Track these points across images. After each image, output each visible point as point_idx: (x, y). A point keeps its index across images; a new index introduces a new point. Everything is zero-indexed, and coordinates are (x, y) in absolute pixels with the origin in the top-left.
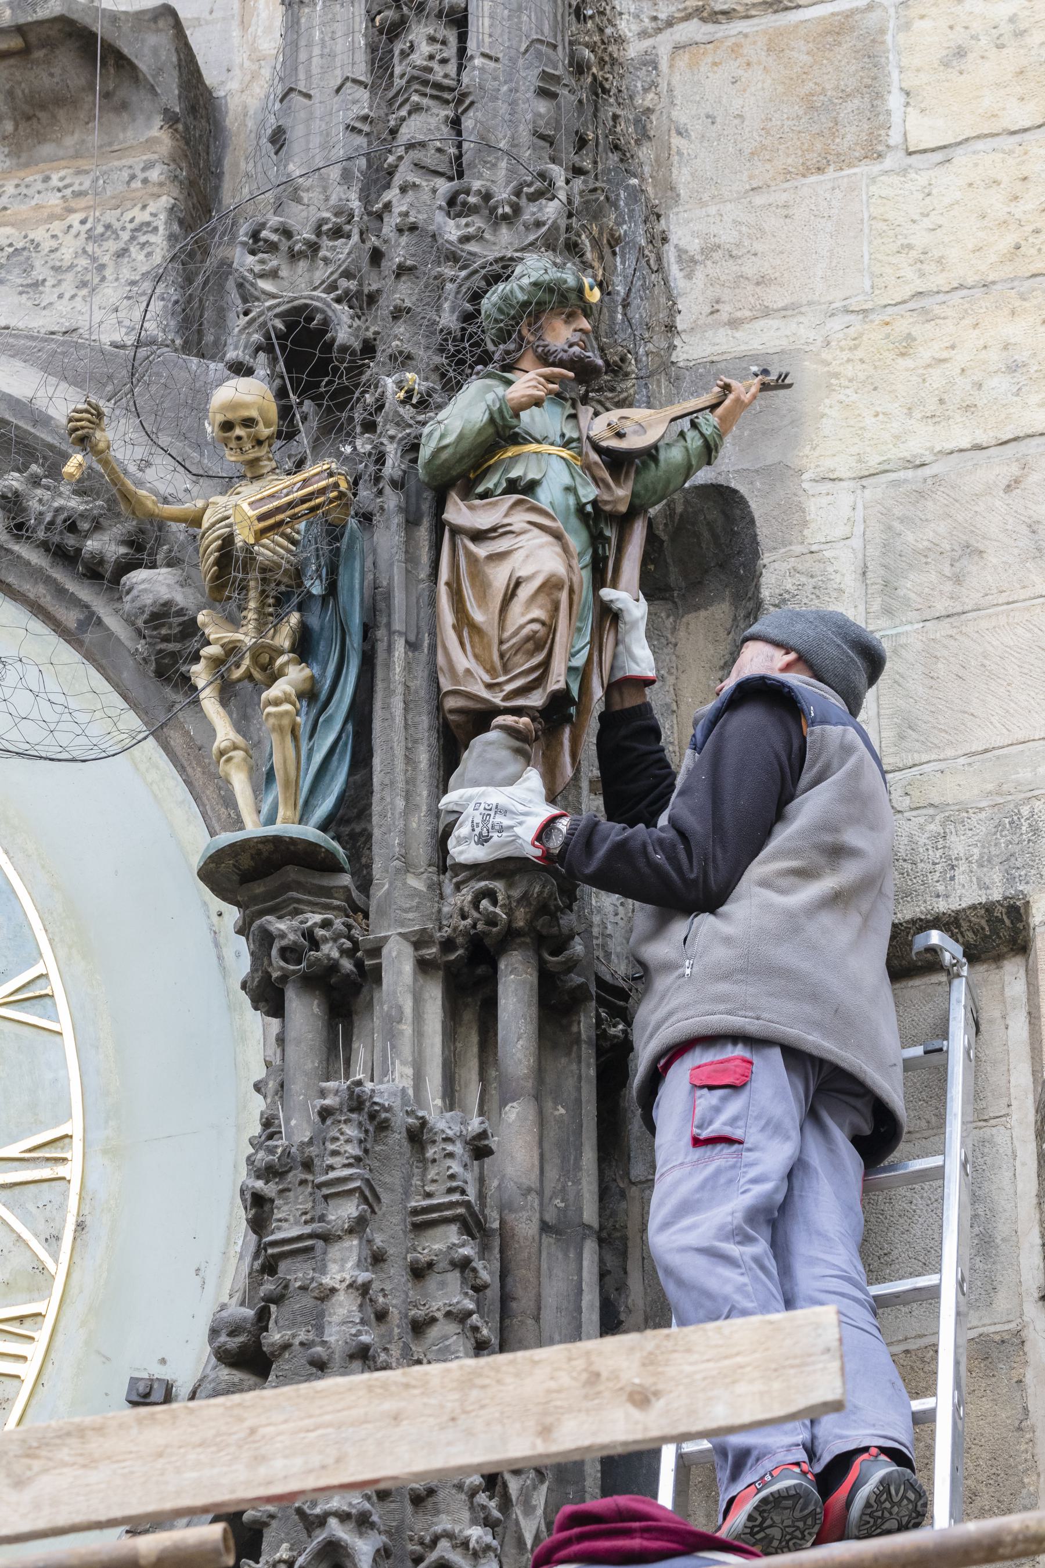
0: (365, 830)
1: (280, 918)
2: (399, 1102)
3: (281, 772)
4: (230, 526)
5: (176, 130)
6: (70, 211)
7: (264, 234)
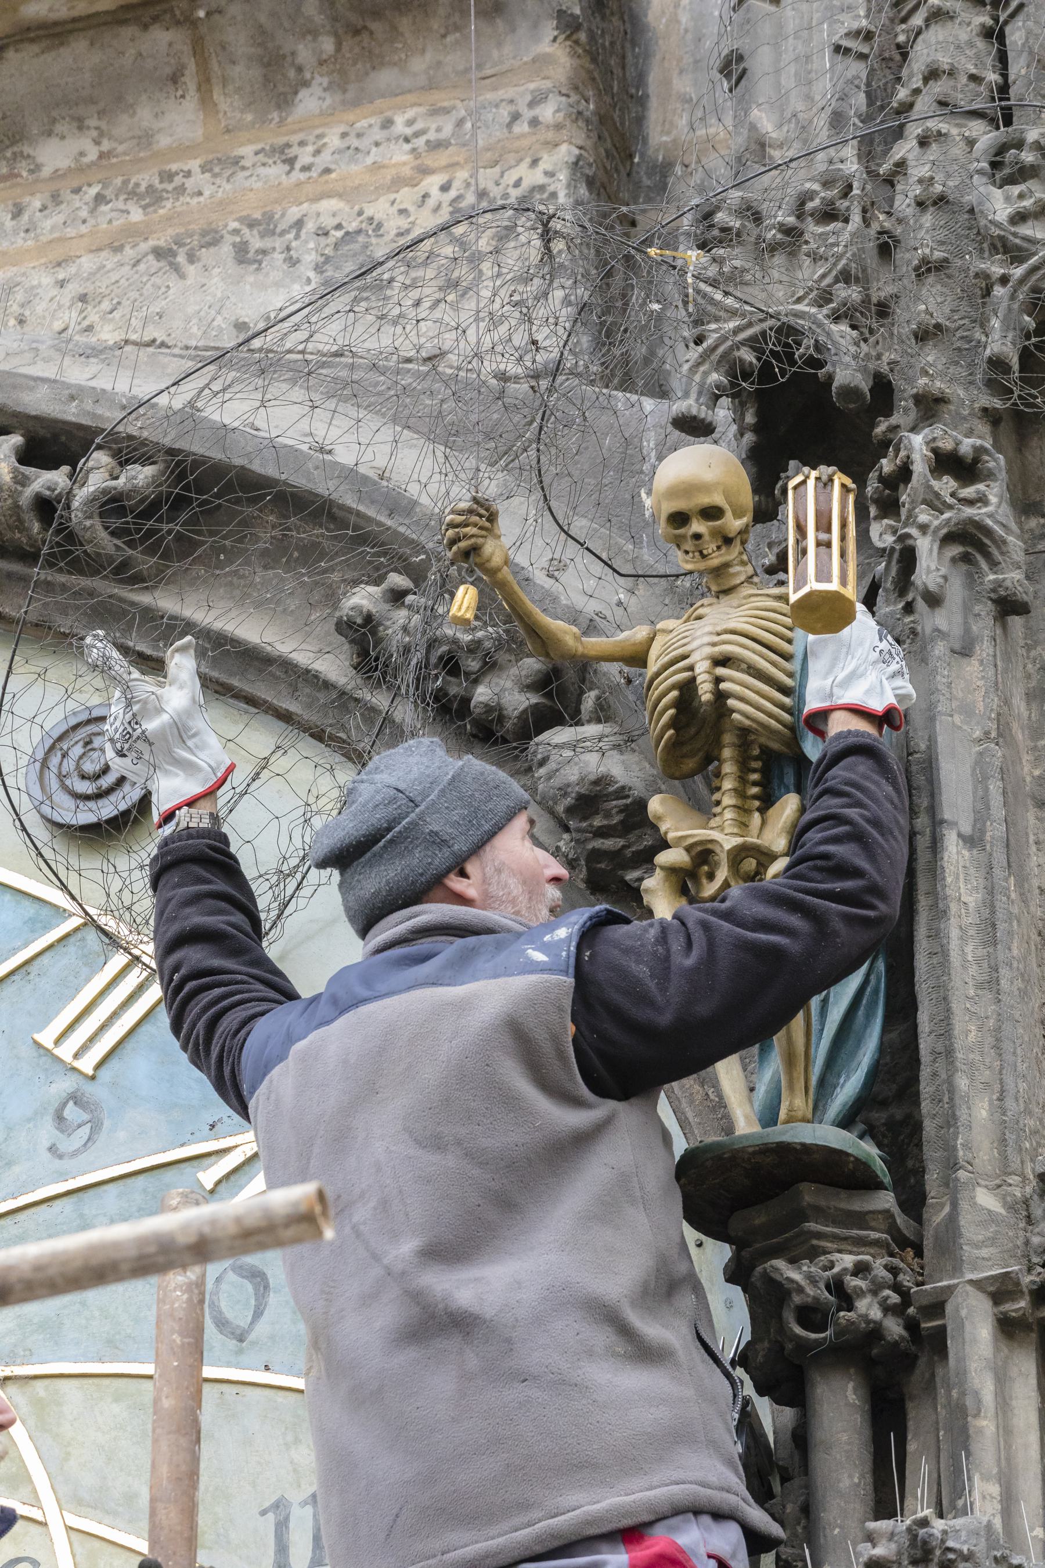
0: (909, 1117)
1: (793, 1261)
2: (983, 1543)
4: (691, 668)
6: (426, 171)
7: (720, 217)
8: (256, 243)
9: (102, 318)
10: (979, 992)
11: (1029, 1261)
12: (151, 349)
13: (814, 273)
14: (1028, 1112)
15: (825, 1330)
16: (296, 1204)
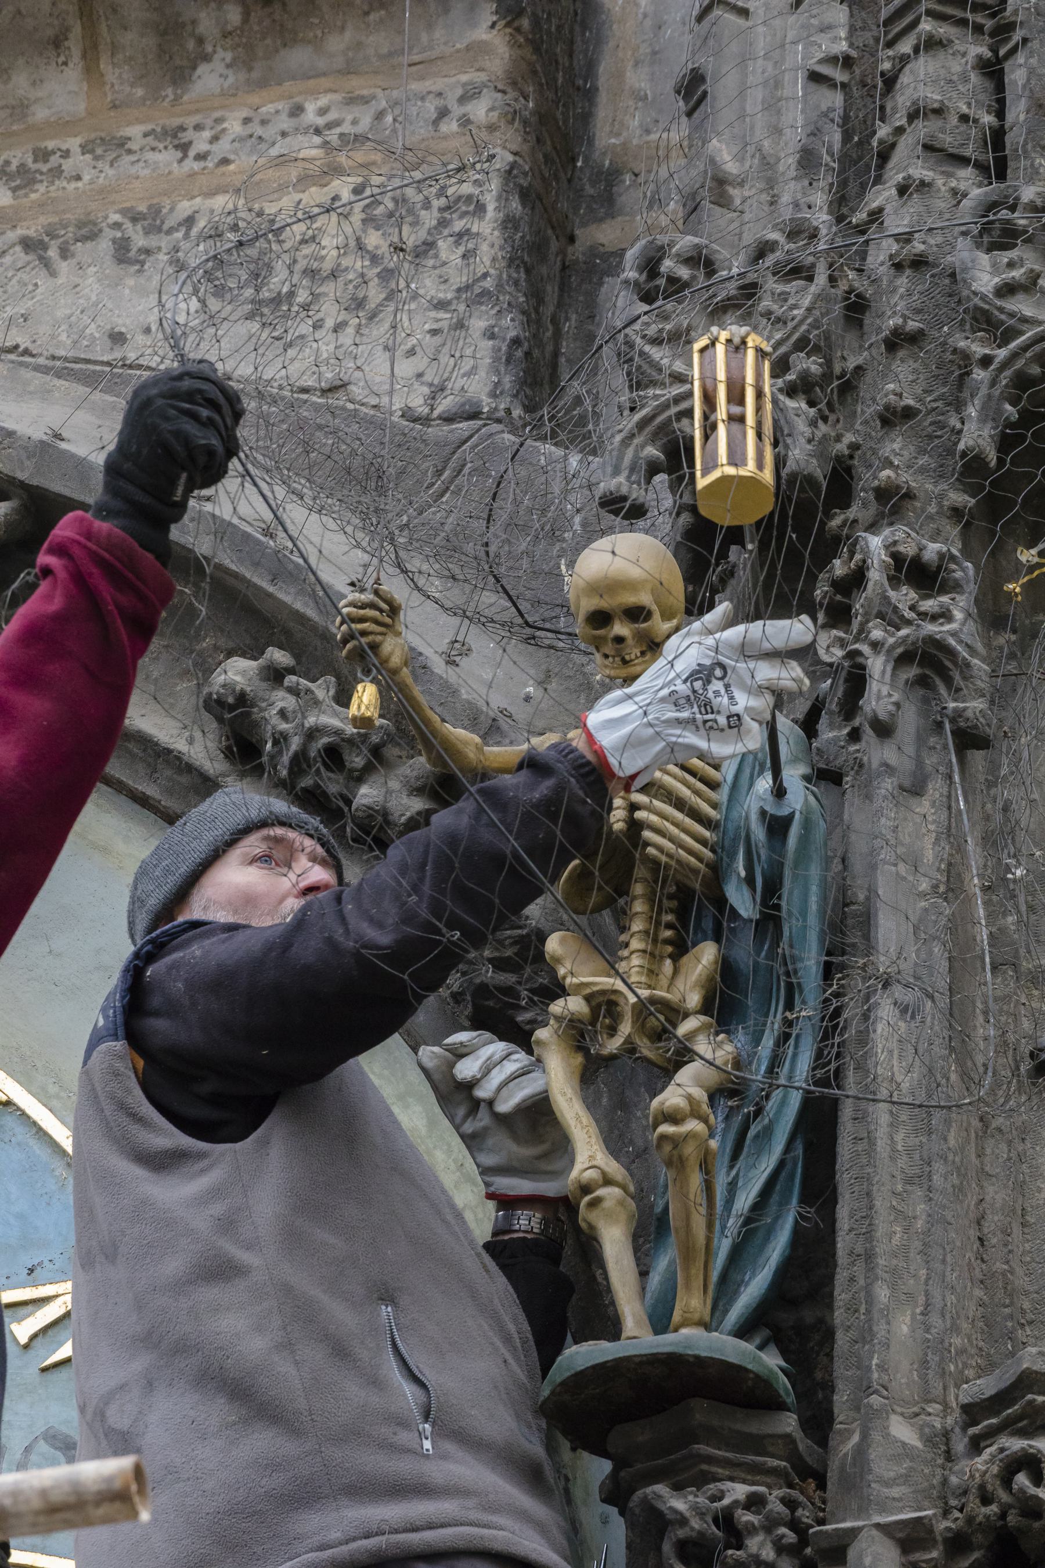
0: (821, 1321)
1: (678, 1487)
5: (518, 30)
6: (335, 171)
7: (667, 265)
8: (140, 241)
10: (908, 1187)
11: (946, 1503)
12: (12, 357)
14: (955, 1329)
16: (110, 1479)
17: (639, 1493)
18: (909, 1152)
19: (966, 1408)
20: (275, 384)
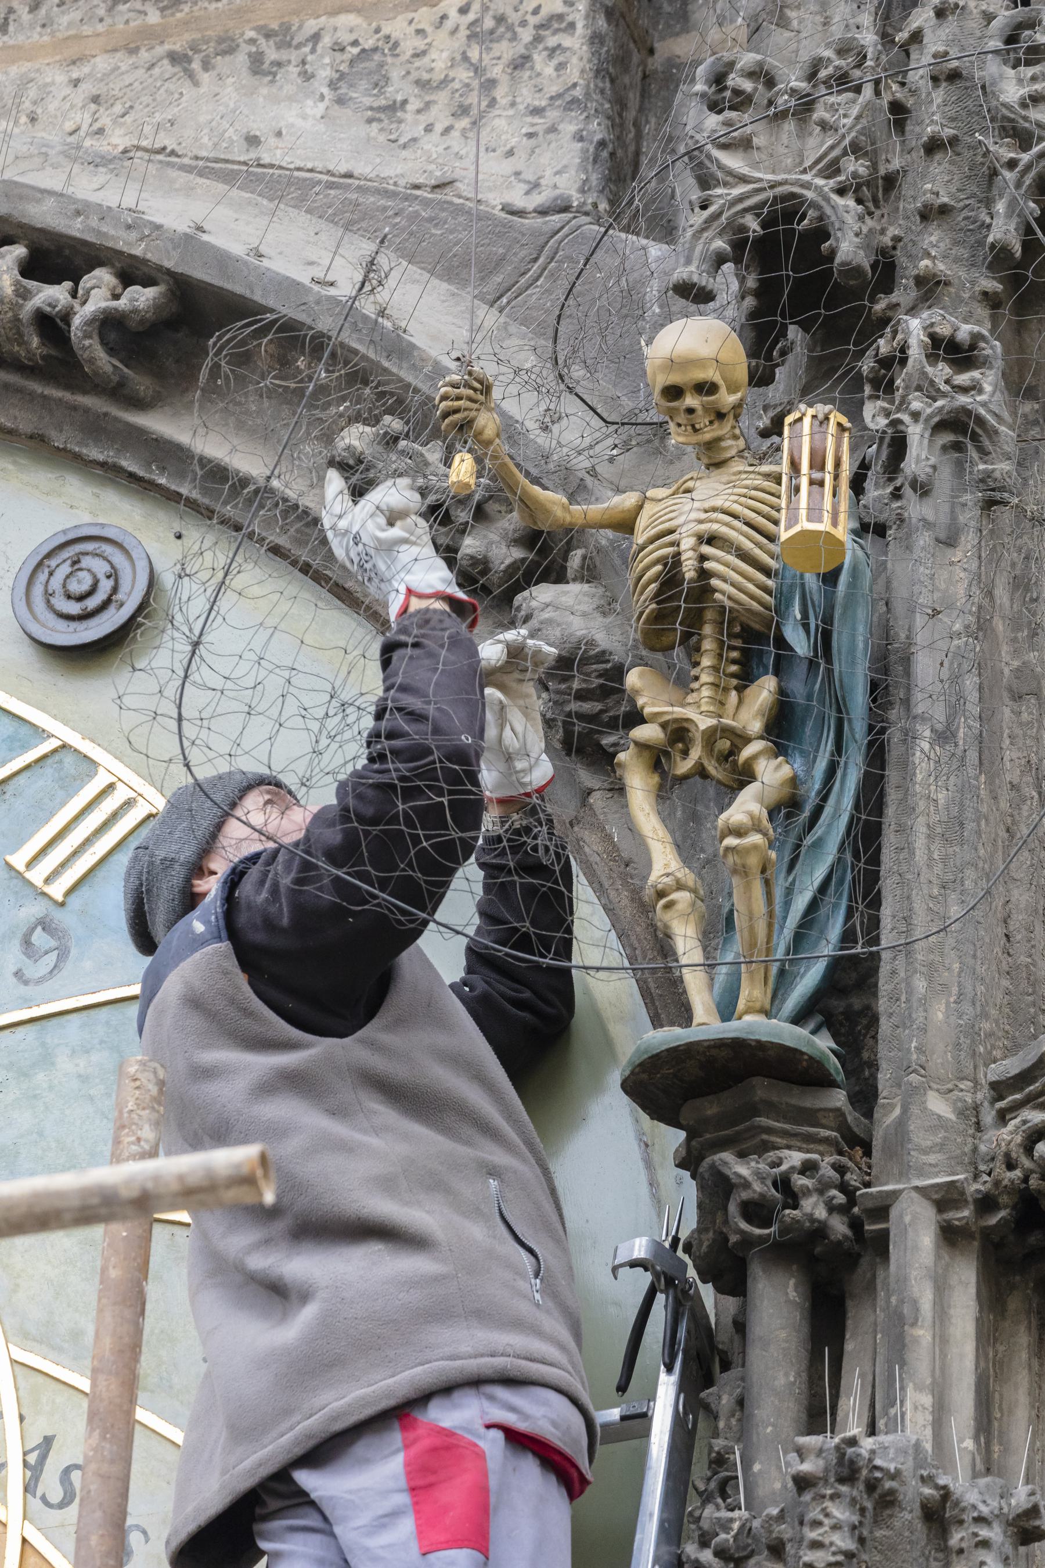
0: (868, 1008)
1: (742, 1155)
2: (910, 1463)
3: (746, 934)
7: (734, 80)
8: (272, 54)
9: (114, 122)
11: (976, 1168)
12: (160, 157)
13: (822, 143)
14: (985, 1015)
15: (767, 1224)
16: (238, 1166)
17: (708, 1160)
18: (945, 860)
19: (994, 1086)
20: (391, 182)
